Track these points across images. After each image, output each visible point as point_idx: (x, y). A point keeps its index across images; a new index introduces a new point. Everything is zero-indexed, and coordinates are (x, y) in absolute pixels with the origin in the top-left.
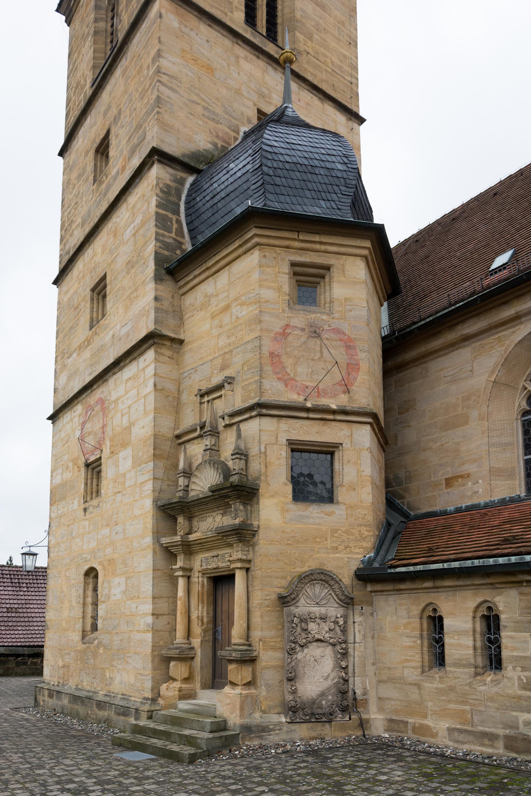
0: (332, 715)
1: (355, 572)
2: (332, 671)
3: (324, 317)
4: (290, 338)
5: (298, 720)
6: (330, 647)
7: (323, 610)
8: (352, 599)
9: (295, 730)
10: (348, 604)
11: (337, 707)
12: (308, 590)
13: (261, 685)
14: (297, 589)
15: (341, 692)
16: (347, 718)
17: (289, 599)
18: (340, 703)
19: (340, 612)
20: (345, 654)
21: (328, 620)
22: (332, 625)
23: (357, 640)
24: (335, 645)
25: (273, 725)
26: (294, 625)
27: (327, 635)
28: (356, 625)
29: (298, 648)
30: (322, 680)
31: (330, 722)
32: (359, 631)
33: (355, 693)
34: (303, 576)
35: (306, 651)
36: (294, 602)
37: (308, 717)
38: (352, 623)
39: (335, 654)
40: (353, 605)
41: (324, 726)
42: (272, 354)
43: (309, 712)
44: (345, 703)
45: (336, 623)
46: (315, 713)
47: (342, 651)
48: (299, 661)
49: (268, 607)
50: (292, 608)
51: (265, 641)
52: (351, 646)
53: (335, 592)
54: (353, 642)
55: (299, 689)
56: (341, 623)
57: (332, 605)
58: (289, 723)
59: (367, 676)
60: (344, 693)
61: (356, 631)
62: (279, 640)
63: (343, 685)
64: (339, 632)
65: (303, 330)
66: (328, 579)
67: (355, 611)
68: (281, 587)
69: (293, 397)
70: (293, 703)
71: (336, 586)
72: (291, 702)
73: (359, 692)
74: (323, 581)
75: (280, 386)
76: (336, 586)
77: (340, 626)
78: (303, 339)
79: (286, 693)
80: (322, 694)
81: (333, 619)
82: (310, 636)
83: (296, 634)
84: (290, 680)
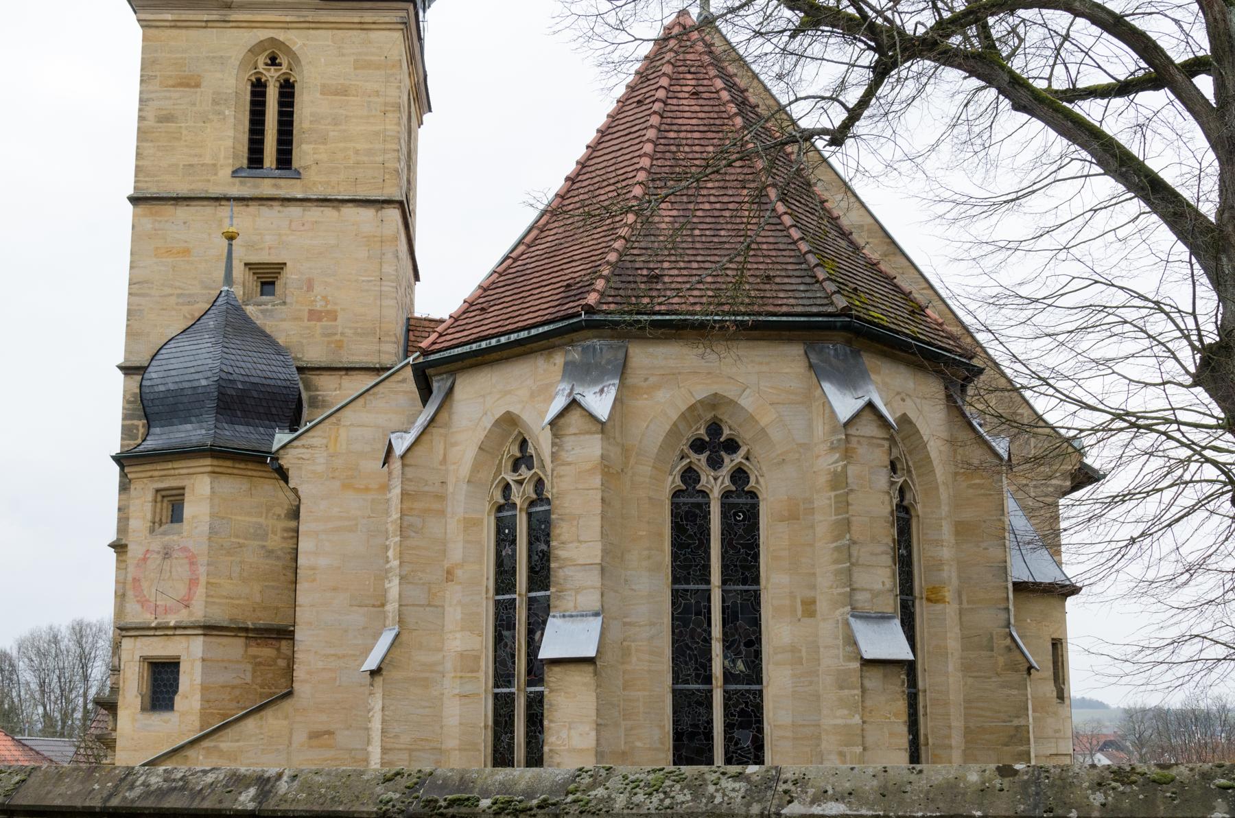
3: (175, 538)
4: (149, 562)
42: (134, 579)
65: (158, 553)
69: (148, 618)
75: (138, 607)
78: (158, 562)
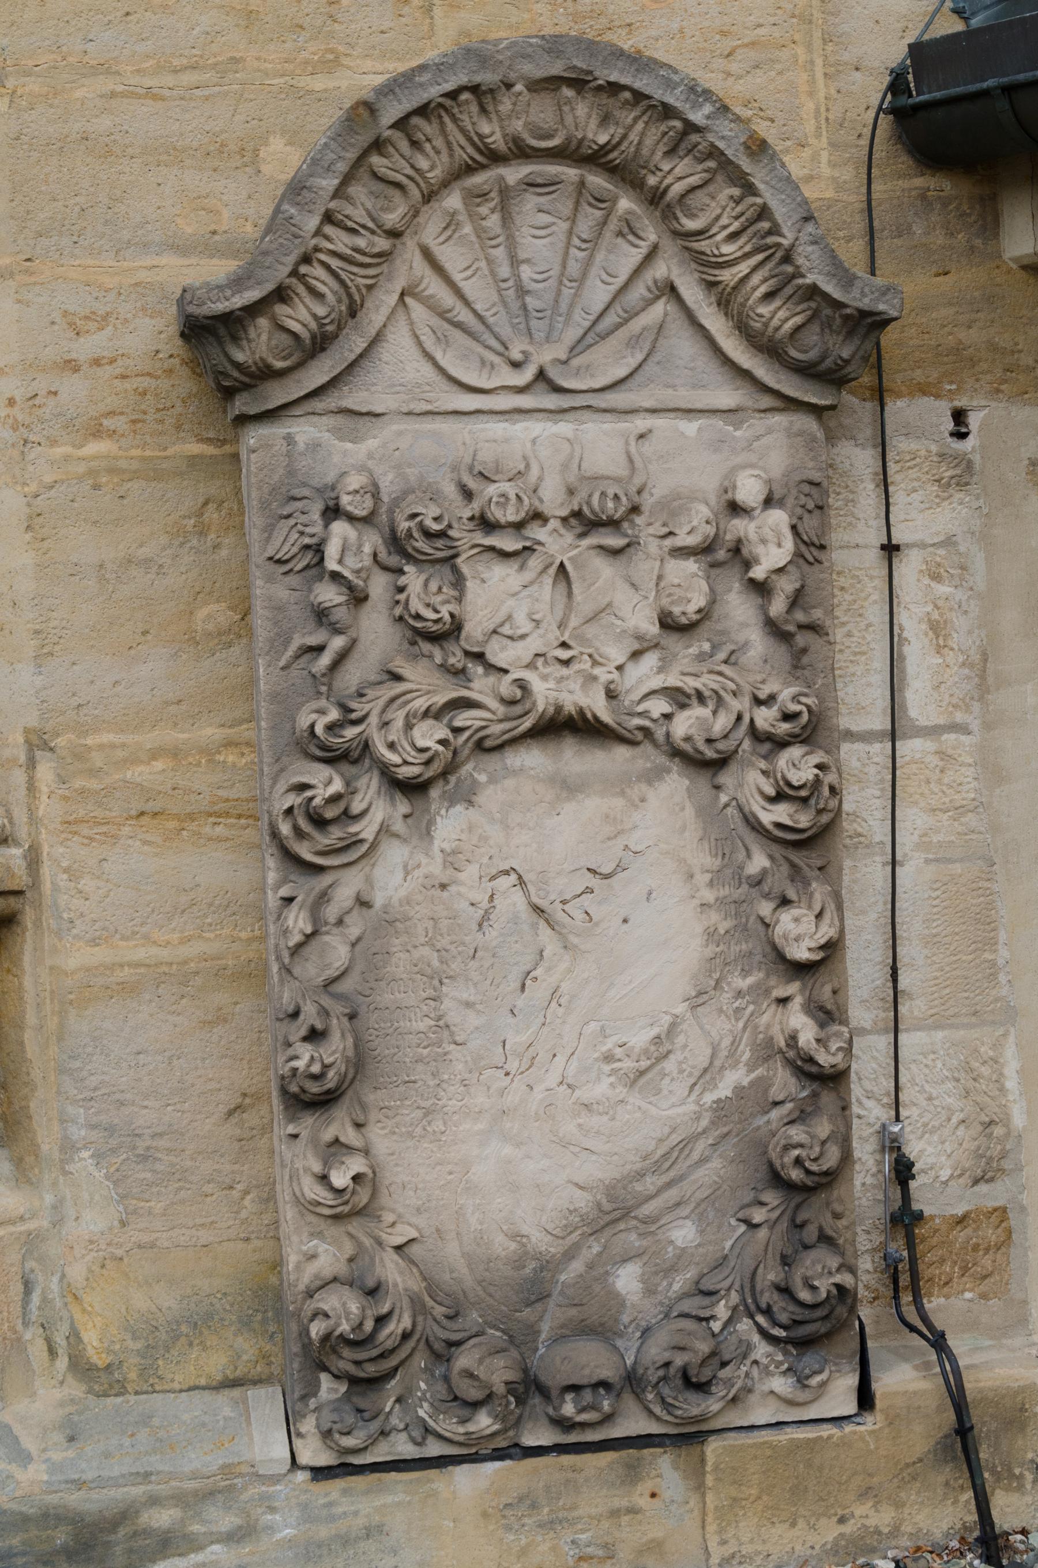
0: (702, 1388)
1: (897, 85)
2: (698, 999)
5: (403, 1447)
6: (677, 783)
7: (599, 445)
8: (869, 324)
9: (370, 1532)
10: (834, 377)
11: (752, 1307)
12: (452, 257)
13: (68, 1148)
14: (341, 241)
15: (777, 1179)
16: (840, 1395)
17: (260, 344)
18: (772, 1275)
19: (764, 452)
20: (809, 844)
21: (646, 529)
22: (689, 586)
23: (920, 704)
24: (721, 763)
25: (179, 1499)
26: (329, 595)
27: (645, 675)
28: (909, 569)
29: (377, 809)
30: (601, 1089)
31: (690, 1437)
32: (937, 628)
33: (903, 1171)
34: (392, 112)
35: (450, 824)
36: (317, 374)
37: (484, 1422)
38: (873, 557)
39: (722, 845)
40: (880, 395)
41: (632, 1474)
43: (499, 1373)
44: (819, 1272)
45: (723, 555)
46: (554, 1380)
47: (782, 813)
48: (390, 922)
49: (97, 432)
50: (304, 430)
51: (80, 755)
52: (861, 763)
53: (706, 264)
54: (880, 722)
55: (393, 1175)
56: (772, 548)
57: (685, 397)
58: (320, 1473)
59: (1010, 1014)
60: (803, 1190)
61: (910, 622)
62: (210, 733)
63: (801, 1117)
64: (757, 643)
66: (645, 137)
67: (900, 445)
68: (208, 246)
70: (344, 1309)
71: (716, 210)
72: (330, 1301)
73: (934, 1155)
74: (595, 158)
76: (716, 210)
77: (761, 589)
79: (289, 1213)
80: (616, 1212)
81: (696, 525)
82: (481, 686)
83: (352, 676)
84: (310, 1099)
